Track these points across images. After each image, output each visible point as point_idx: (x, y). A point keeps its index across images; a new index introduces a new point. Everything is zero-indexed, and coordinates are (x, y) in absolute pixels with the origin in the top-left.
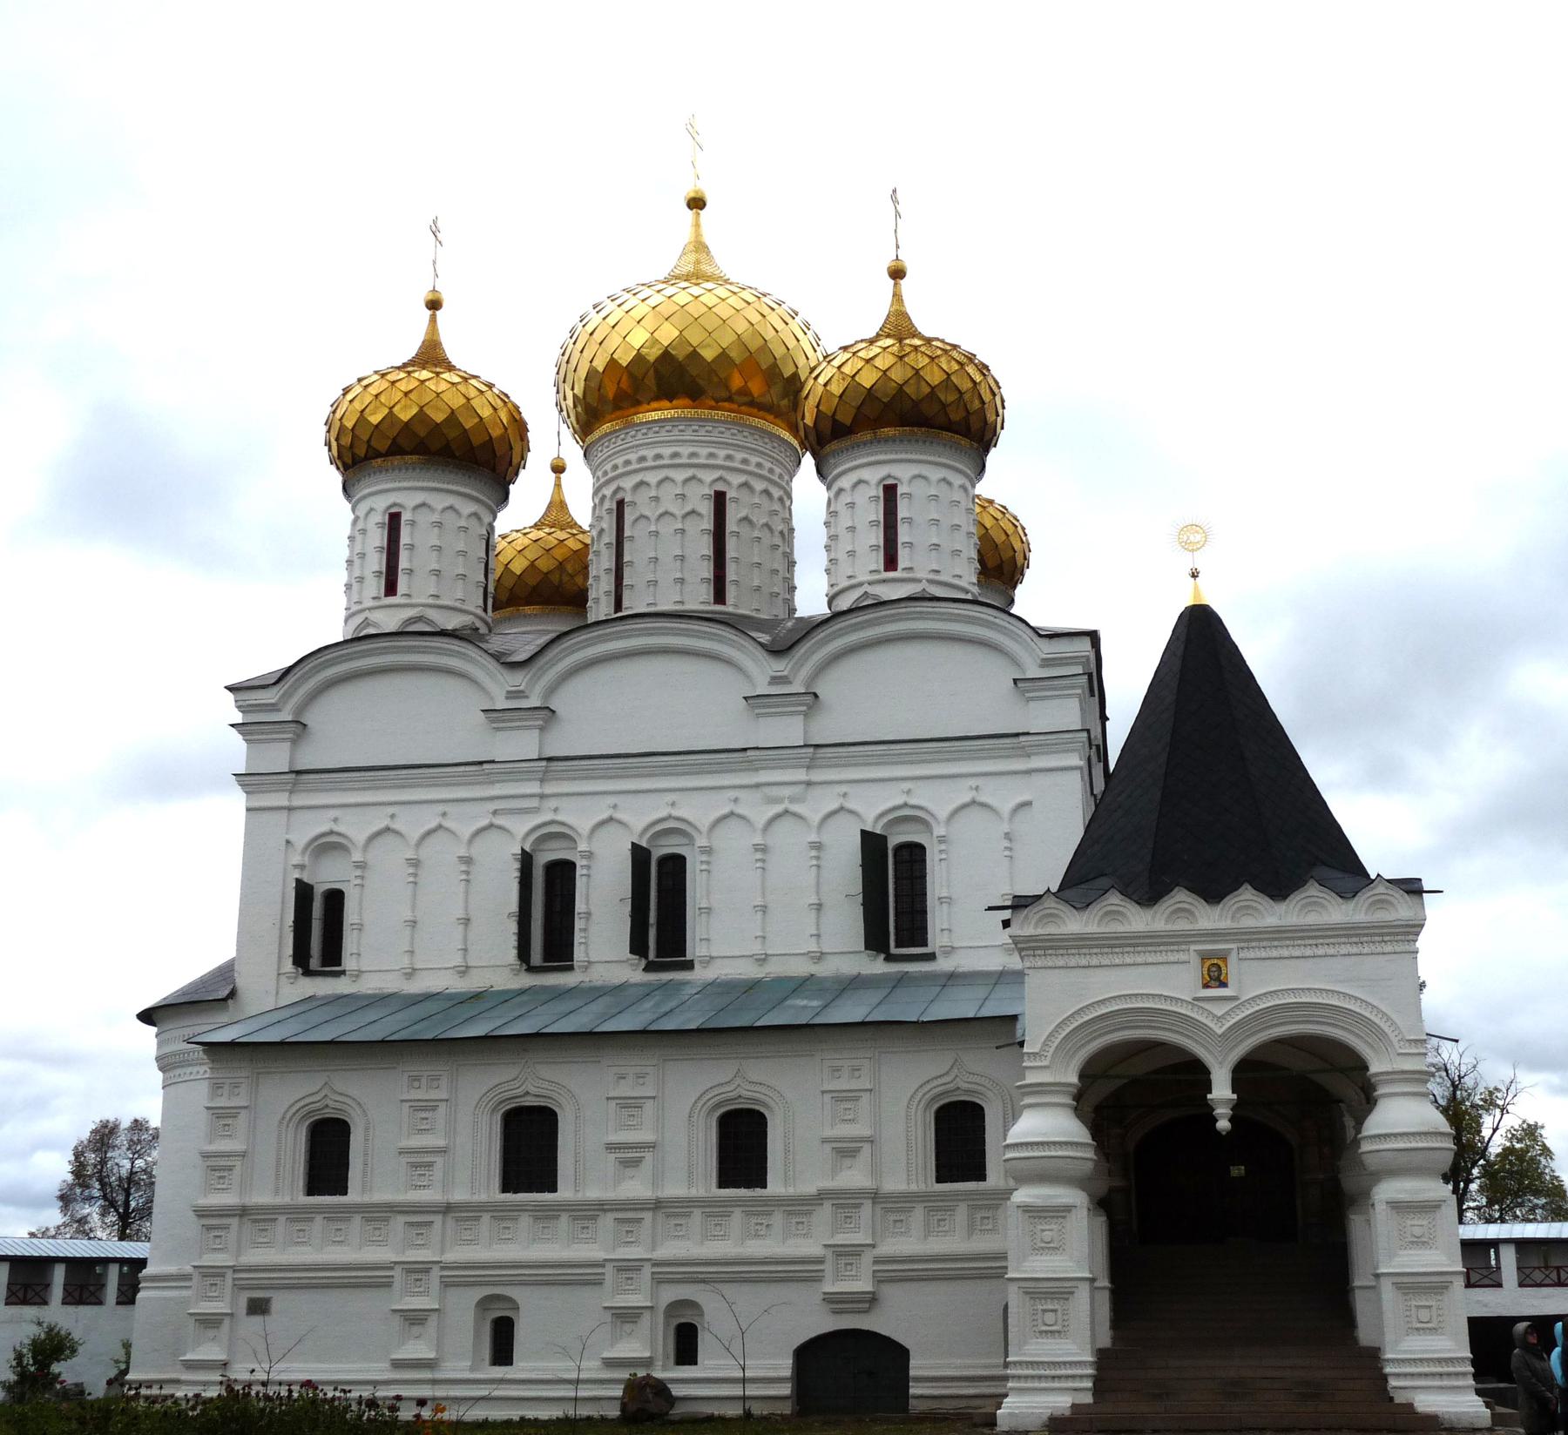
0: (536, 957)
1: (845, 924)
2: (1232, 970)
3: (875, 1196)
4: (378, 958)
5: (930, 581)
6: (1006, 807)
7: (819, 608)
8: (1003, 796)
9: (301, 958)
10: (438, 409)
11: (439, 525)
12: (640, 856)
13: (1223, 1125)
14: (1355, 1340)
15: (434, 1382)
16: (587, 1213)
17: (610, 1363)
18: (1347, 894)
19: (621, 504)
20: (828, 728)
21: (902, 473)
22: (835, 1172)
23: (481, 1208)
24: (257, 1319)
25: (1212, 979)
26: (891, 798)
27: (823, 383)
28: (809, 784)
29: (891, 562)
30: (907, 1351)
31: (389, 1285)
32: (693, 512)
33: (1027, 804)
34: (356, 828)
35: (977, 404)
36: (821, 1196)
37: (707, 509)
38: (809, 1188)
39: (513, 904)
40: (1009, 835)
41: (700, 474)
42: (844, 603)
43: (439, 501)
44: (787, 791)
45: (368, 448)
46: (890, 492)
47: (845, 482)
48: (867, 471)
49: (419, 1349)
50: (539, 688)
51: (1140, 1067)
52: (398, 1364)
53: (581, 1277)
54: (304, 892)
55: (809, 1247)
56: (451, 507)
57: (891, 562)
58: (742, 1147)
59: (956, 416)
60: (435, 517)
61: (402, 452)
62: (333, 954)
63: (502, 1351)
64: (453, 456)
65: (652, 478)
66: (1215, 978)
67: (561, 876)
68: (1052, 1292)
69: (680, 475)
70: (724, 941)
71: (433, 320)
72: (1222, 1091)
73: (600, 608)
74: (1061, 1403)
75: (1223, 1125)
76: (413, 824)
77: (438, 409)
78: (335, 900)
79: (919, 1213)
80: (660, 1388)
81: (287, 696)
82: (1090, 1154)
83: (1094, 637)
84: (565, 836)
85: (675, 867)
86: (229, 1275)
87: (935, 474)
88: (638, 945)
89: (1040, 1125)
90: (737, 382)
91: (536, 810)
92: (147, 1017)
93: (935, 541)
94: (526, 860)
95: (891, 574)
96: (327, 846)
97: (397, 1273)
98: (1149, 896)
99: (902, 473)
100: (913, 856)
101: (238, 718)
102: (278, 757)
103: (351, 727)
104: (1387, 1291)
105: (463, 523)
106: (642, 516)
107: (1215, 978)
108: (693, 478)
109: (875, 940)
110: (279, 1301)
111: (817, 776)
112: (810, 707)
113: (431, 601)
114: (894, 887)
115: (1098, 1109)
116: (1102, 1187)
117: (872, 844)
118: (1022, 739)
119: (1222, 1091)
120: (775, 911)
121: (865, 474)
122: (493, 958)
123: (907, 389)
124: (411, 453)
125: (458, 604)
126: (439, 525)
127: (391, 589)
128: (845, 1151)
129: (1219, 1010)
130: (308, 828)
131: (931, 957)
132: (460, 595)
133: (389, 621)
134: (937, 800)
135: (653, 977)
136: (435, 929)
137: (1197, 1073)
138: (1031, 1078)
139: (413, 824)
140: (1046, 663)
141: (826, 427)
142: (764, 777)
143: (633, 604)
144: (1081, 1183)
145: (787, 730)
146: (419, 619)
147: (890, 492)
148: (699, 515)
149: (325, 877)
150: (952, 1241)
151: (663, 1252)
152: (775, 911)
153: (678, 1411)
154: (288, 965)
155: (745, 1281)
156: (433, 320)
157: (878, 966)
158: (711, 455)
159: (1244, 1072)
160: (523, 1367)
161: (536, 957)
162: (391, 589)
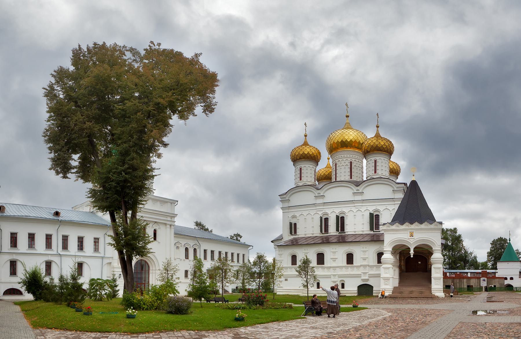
0: (323, 232)
3: (369, 266)
9: (291, 233)
27: (366, 145)
29: (375, 172)
34: (297, 214)
42: (368, 178)
47: (369, 160)
54: (291, 224)
57: (375, 172)
67: (326, 220)
73: (333, 180)
79: (375, 268)
84: (327, 214)
90: (353, 144)
102: (286, 205)
120: (357, 224)
121: (371, 159)
139: (305, 213)
141: (366, 151)
142: (356, 205)
143: (338, 179)
149: (293, 222)
152: (357, 224)
161: (323, 232)
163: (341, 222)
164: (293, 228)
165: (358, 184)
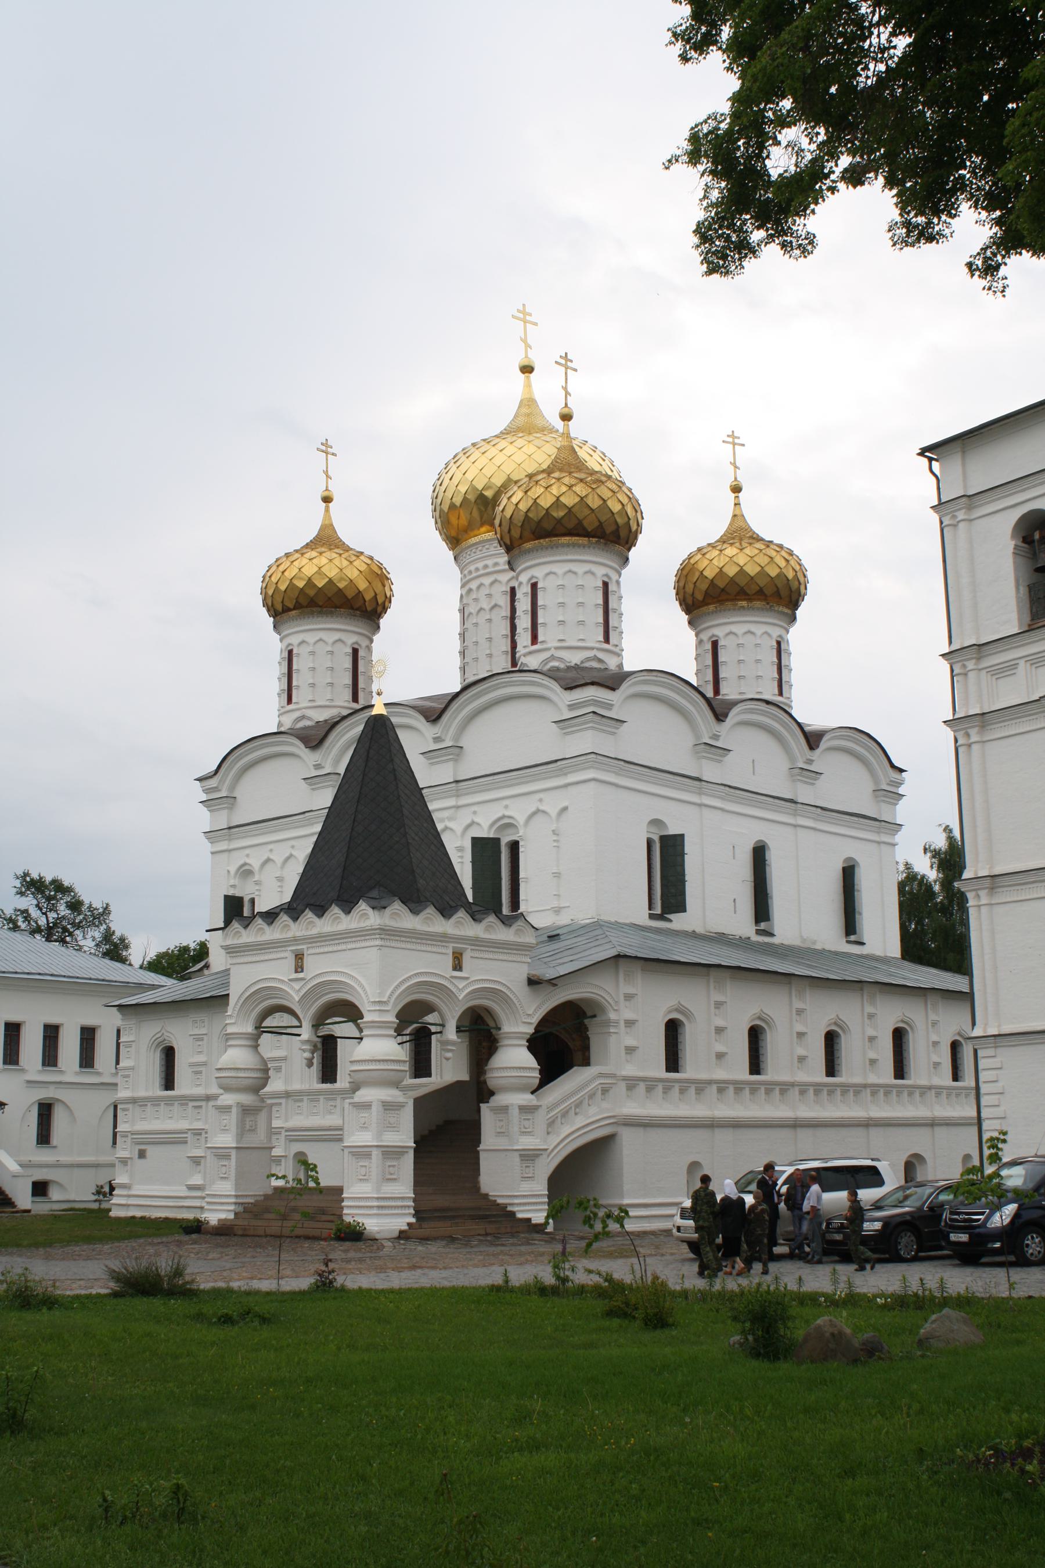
5: (557, 648)
6: (553, 812)
8: (552, 804)
10: (301, 579)
11: (312, 653)
14: (476, 1187)
15: (129, 1196)
23: (309, 1093)
24: (142, 1161)
26: (496, 811)
28: (458, 807)
31: (186, 1142)
32: (496, 606)
33: (565, 809)
37: (504, 601)
43: (311, 638)
45: (294, 603)
49: (197, 1180)
50: (329, 761)
52: (191, 1188)
56: (321, 640)
59: (570, 525)
60: (311, 649)
61: (289, 610)
64: (317, 605)
69: (487, 581)
71: (327, 509)
77: (301, 579)
86: (284, 1134)
87: (560, 569)
93: (561, 618)
95: (535, 647)
96: (245, 872)
97: (189, 1135)
98: (348, 905)
99: (539, 573)
101: (204, 797)
105: (329, 648)
106: (481, 609)
108: (496, 581)
110: (150, 1150)
111: (462, 801)
112: (458, 755)
113: (310, 704)
118: (559, 763)
123: (531, 515)
124: (294, 609)
125: (328, 703)
126: (312, 653)
130: (238, 860)
132: (329, 697)
134: (519, 812)
140: (571, 707)
146: (303, 717)
148: (500, 606)
151: (290, 1124)
155: (330, 1140)
156: (327, 509)
158: (496, 564)
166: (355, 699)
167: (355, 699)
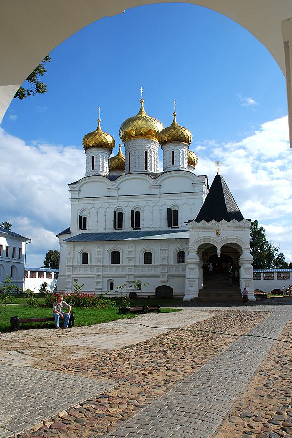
0: (116, 228)
1: (165, 222)
2: (222, 233)
4: (92, 228)
7: (161, 170)
9: (80, 228)
12: (133, 211)
13: (219, 256)
16: (124, 267)
17: (128, 290)
18: (239, 221)
19: (130, 153)
20: (163, 190)
21: (174, 148)
22: (162, 262)
23: (108, 266)
25: (219, 234)
29: (173, 164)
30: (156, 289)
35: (187, 137)
36: (160, 265)
38: (158, 264)
39: (113, 219)
40: (190, 209)
41: (143, 148)
44: (155, 201)
46: (173, 152)
47: (167, 150)
48: (170, 148)
51: (207, 247)
52: (96, 289)
53: (123, 277)
54: (80, 217)
55: (158, 273)
57: (173, 164)
58: (148, 258)
62: (85, 227)
63: (112, 288)
65: (134, 149)
66: (219, 234)
67: (120, 214)
68: (194, 280)
69: (139, 148)
70: (145, 225)
72: (219, 252)
73: (127, 170)
74: (193, 297)
75: (219, 256)
76: (97, 206)
78: (85, 218)
80: (135, 293)
81: (77, 186)
82: (199, 260)
83: (206, 176)
85: (138, 213)
88: (132, 226)
89: (192, 256)
91: (116, 204)
92: (57, 236)
94: (115, 212)
100: (176, 212)
103: (87, 190)
104: (242, 280)
107: (219, 234)
109: (170, 225)
110: (78, 279)
114: (173, 217)
115: (203, 253)
116: (202, 265)
117: (169, 210)
119: (219, 252)
120: (153, 219)
122: (110, 228)
127: (93, 169)
128: (163, 259)
129: (219, 238)
131: (179, 228)
133: (93, 173)
135: (134, 231)
136: (101, 223)
137: (215, 248)
138: (190, 248)
141: (163, 141)
142: (152, 199)
144: (197, 264)
145: (156, 191)
147: (173, 152)
149: (84, 214)
150: (181, 273)
152: (153, 219)
153: (138, 296)
154: (78, 228)
157: (170, 229)
159: (222, 248)
160: (115, 290)
162: (93, 169)
163: (136, 217)
164: (83, 222)
165: (156, 176)
166: (129, 170)
167: (129, 170)
